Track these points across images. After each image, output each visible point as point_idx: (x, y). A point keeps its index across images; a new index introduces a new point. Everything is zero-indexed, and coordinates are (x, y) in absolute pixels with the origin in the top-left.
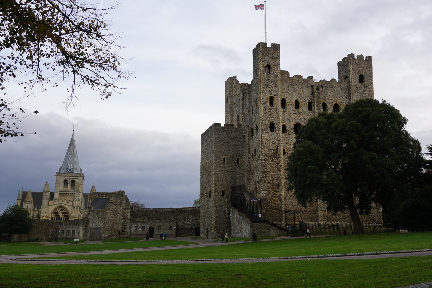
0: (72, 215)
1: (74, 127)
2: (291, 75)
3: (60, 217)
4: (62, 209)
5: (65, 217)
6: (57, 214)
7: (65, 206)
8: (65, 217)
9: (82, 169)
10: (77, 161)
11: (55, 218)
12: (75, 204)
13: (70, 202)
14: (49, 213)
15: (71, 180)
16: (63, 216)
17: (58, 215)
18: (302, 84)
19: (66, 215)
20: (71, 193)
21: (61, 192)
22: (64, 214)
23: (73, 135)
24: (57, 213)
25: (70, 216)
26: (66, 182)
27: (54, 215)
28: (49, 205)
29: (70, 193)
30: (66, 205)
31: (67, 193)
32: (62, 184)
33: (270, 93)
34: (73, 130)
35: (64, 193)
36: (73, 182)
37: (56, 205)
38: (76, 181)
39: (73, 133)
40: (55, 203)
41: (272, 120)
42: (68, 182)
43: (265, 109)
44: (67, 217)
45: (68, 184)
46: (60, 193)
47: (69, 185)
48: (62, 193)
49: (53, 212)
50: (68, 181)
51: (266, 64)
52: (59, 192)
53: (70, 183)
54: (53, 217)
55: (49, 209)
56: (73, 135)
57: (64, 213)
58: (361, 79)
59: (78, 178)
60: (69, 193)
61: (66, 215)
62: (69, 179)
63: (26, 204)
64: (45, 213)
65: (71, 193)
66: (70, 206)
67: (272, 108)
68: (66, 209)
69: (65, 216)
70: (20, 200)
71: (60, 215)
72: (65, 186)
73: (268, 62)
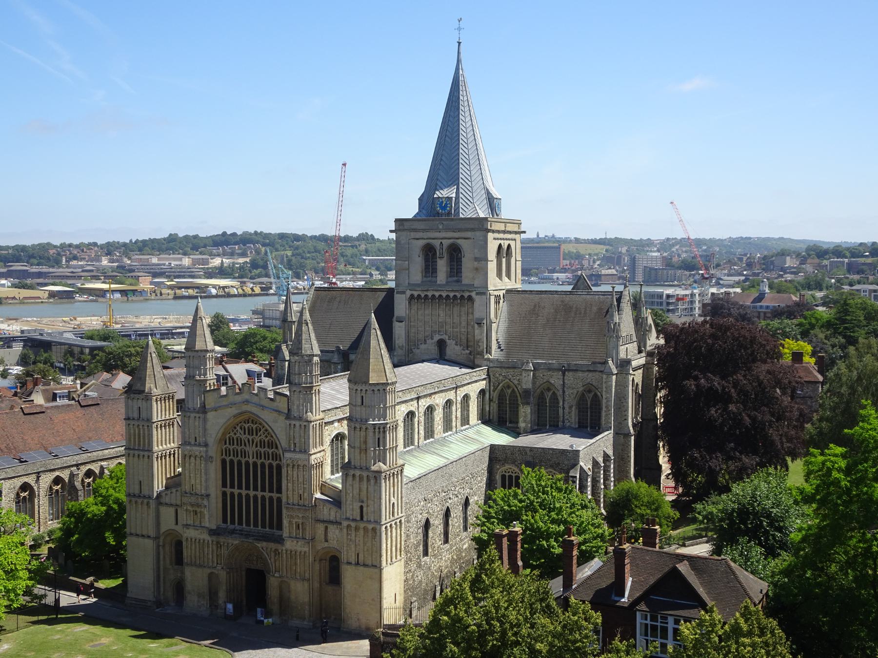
0: (288, 455)
1: (459, 29)
3: (251, 461)
4: (254, 427)
5: (267, 463)
6: (239, 449)
7: (266, 416)
8: (267, 463)
9: (495, 193)
10: (474, 169)
11: (232, 462)
12: (298, 406)
13: (278, 397)
14: (211, 441)
15: (446, 243)
16: (258, 455)
17: (244, 454)
19: (270, 451)
20: (448, 296)
22: (262, 450)
23: (459, 61)
24: (240, 442)
25: (284, 461)
26: (429, 252)
27: (227, 452)
28: (207, 407)
29: (444, 294)
30: (263, 407)
31: (437, 294)
32: (418, 263)
34: (459, 43)
35: (426, 296)
36: (455, 253)
37: (229, 410)
39: (459, 53)
40: (225, 402)
44: (275, 464)
45: (438, 260)
46: (412, 296)
47: (442, 266)
48: (419, 296)
49: (226, 439)
52: (409, 293)
53: (445, 255)
54: (228, 459)
55: (209, 425)
56: (459, 61)
57: (262, 444)
59: (469, 234)
60: (440, 296)
61: (270, 451)
63: (135, 401)
64: (193, 442)
65: (448, 296)
66: (279, 412)
69: (266, 456)
71: (251, 450)
72: (430, 268)
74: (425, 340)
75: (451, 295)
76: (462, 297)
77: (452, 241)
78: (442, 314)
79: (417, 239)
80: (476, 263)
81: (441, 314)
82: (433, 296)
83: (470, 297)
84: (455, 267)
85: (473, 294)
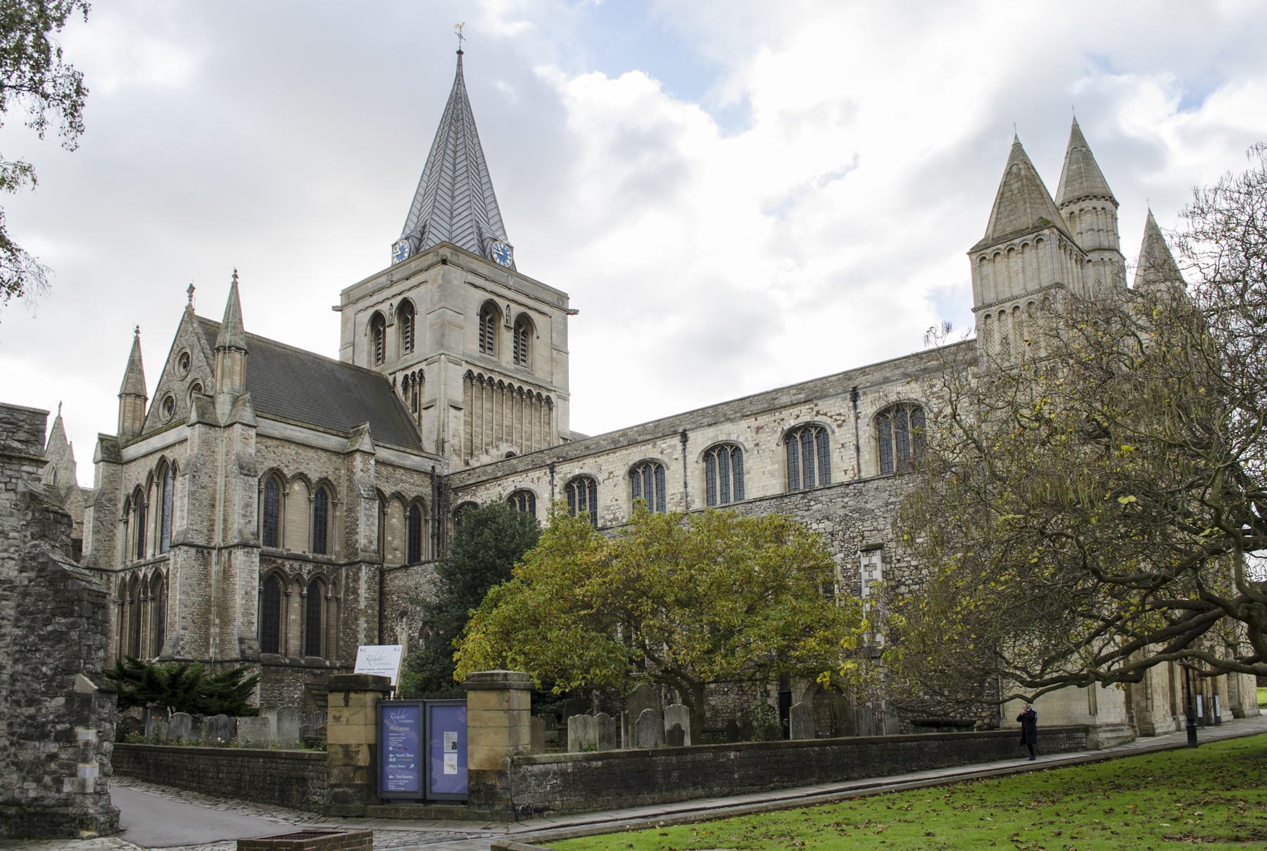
15: (516, 310)
21: (476, 371)
26: (489, 312)
31: (506, 381)
35: (491, 379)
36: (523, 326)
42: (503, 322)
45: (503, 330)
46: (470, 373)
47: (507, 339)
50: (504, 313)
52: (466, 367)
53: (512, 325)
65: (520, 388)
70: (237, 356)
72: (487, 341)
74: (487, 452)
75: (526, 388)
76: (539, 395)
77: (523, 309)
78: (506, 411)
79: (476, 287)
80: (554, 352)
81: (506, 414)
82: (501, 382)
83: (548, 399)
84: (521, 353)
85: (552, 395)
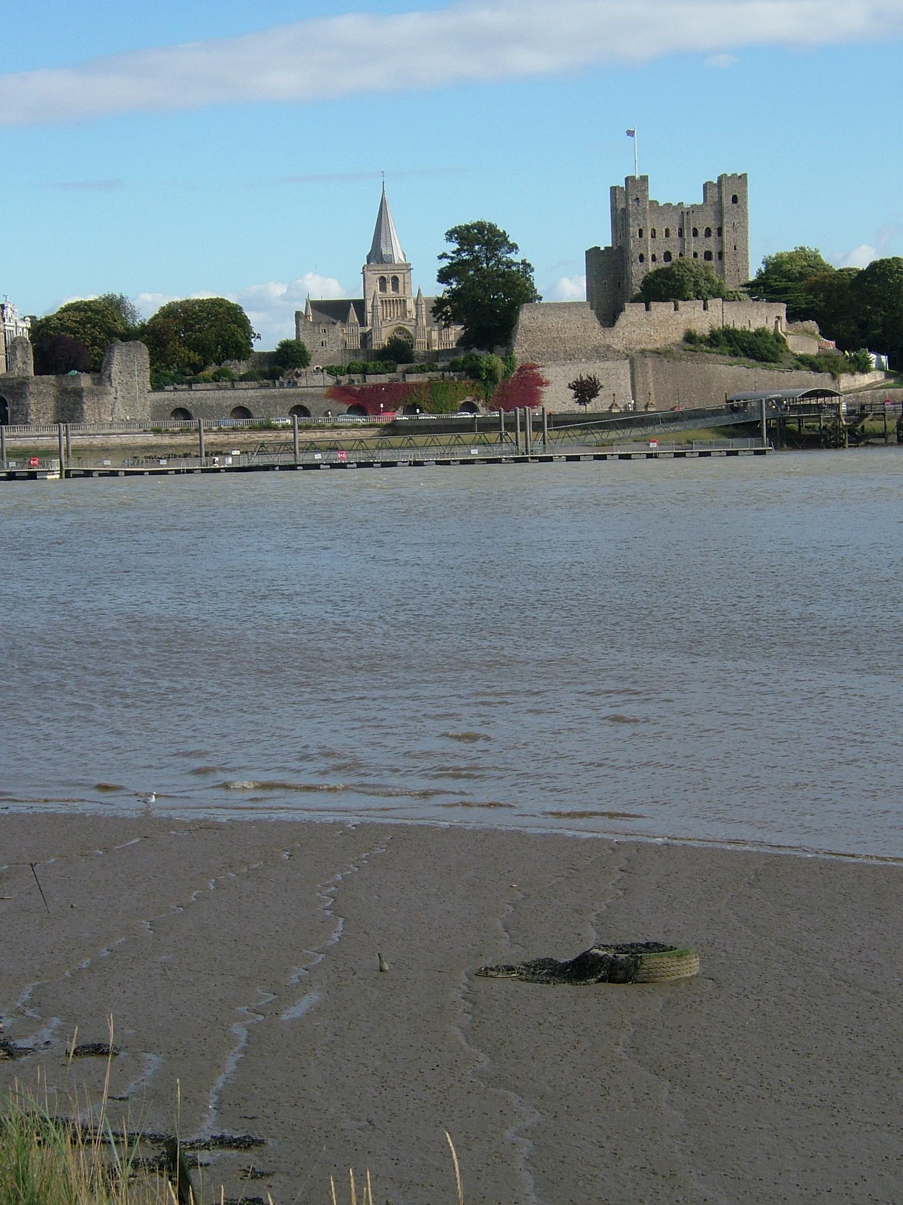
2: (661, 204)
7: (406, 327)
15: (391, 276)
18: (672, 212)
26: (383, 280)
33: (639, 225)
36: (395, 279)
38: (400, 277)
40: (390, 324)
41: (641, 251)
43: (634, 241)
47: (389, 286)
51: (635, 197)
58: (735, 199)
62: (388, 276)
67: (640, 239)
68: (408, 332)
72: (383, 288)
73: (636, 195)
84: (395, 287)
